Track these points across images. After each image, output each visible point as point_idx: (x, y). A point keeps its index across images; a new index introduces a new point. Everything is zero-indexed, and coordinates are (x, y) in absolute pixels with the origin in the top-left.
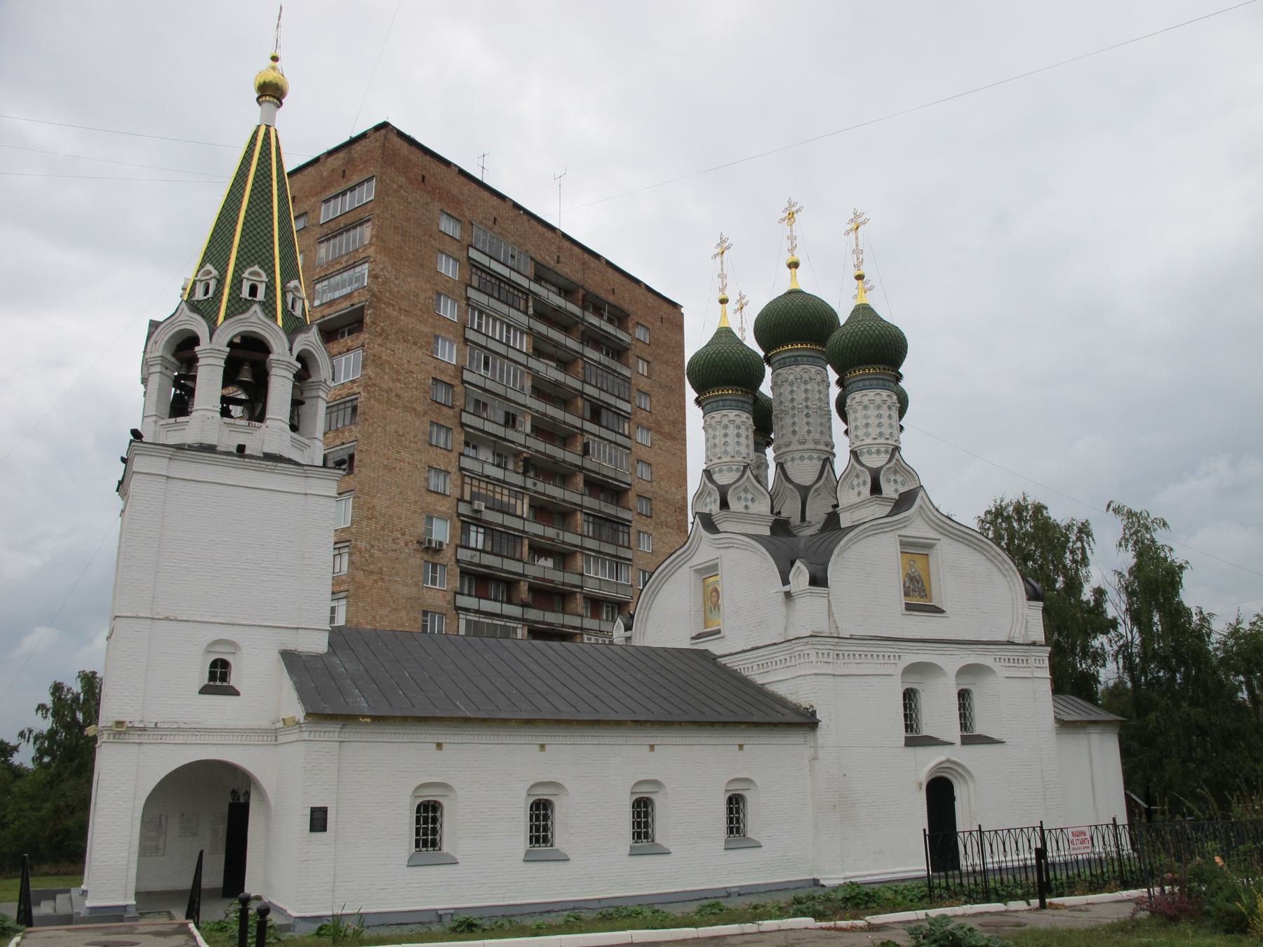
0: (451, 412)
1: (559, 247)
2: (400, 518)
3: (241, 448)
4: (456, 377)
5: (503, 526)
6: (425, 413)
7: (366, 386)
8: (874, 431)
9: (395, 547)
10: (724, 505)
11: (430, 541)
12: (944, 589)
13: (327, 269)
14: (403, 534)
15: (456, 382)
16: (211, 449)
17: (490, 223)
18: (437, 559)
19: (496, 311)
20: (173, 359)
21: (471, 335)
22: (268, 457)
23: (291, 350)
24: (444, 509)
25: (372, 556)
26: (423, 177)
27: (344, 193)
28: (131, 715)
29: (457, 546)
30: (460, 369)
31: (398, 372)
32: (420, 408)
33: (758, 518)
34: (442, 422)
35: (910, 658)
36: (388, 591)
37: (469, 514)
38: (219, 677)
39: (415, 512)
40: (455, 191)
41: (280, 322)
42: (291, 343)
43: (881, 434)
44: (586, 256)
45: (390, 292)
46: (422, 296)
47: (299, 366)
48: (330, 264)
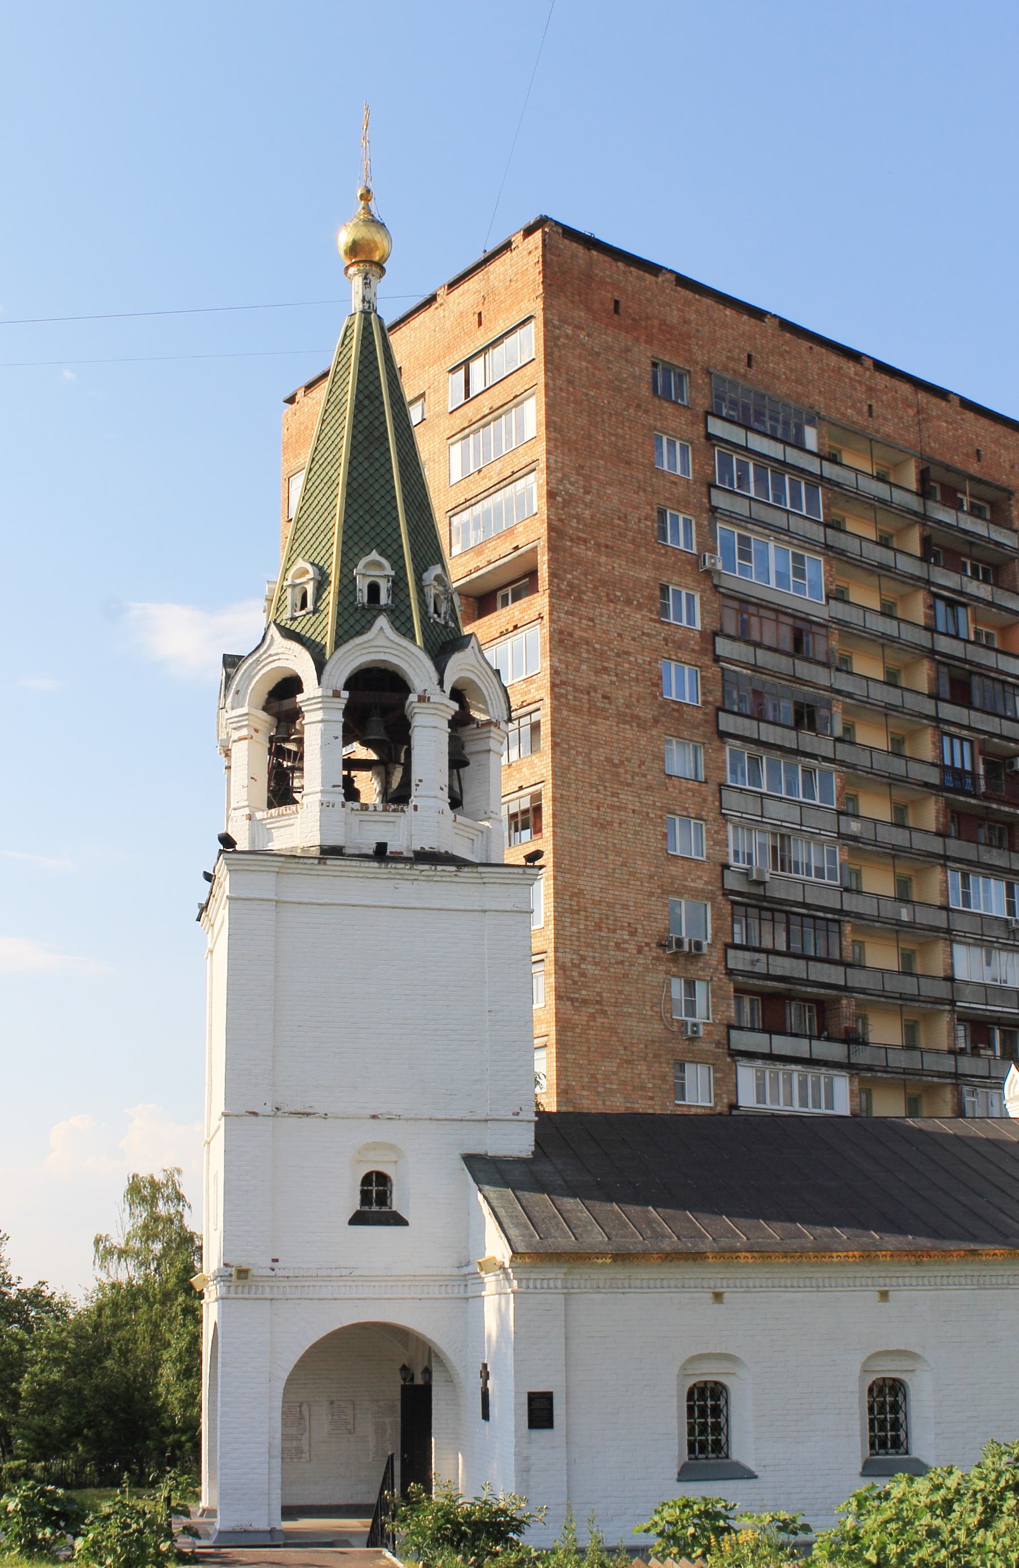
1: (870, 389)
2: (625, 907)
3: (381, 847)
4: (703, 652)
5: (804, 905)
6: (656, 721)
9: (620, 956)
11: (679, 943)
14: (633, 933)
15: (707, 661)
17: (742, 368)
18: (693, 970)
20: (264, 715)
23: (441, 683)
24: (699, 884)
25: (583, 974)
26: (617, 303)
31: (602, 654)
32: (646, 713)
36: (613, 1031)
37: (744, 888)
38: (377, 1202)
39: (651, 894)
40: (674, 317)
41: (419, 640)
42: (441, 670)
44: (922, 397)
45: (579, 518)
46: (634, 517)
47: (456, 706)
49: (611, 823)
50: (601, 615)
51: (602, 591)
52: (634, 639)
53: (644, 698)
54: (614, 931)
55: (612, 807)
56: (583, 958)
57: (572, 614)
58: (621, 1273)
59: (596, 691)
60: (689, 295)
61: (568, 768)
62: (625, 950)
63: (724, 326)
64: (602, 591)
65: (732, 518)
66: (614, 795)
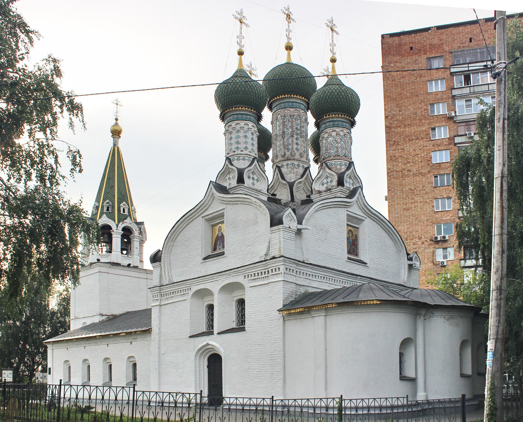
2: (418, 231)
4: (450, 144)
6: (429, 172)
24: (449, 218)
32: (426, 171)
34: (442, 173)
39: (427, 225)
49: (411, 208)
50: (407, 146)
51: (407, 139)
52: (420, 149)
53: (424, 166)
54: (413, 240)
55: (411, 203)
57: (395, 150)
59: (405, 170)
60: (443, 30)
61: (394, 196)
62: (417, 244)
63: (459, 33)
65: (461, 97)
66: (412, 199)
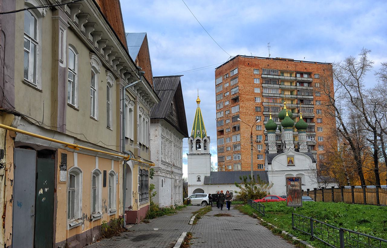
0: (261, 113)
3: (198, 154)
4: (261, 105)
7: (240, 113)
8: (287, 138)
10: (268, 149)
11: (257, 141)
12: (296, 162)
13: (232, 87)
16: (195, 154)
17: (267, 67)
19: (270, 87)
21: (264, 94)
22: (202, 154)
24: (261, 133)
27: (233, 70)
28: (190, 184)
29: (264, 140)
30: (262, 103)
32: (253, 114)
33: (275, 150)
34: (259, 116)
35: (287, 173)
38: (199, 179)
40: (257, 63)
43: (288, 138)
48: (233, 86)
51: (247, 100)
56: (245, 144)
58: (211, 185)
63: (264, 62)
64: (247, 100)
